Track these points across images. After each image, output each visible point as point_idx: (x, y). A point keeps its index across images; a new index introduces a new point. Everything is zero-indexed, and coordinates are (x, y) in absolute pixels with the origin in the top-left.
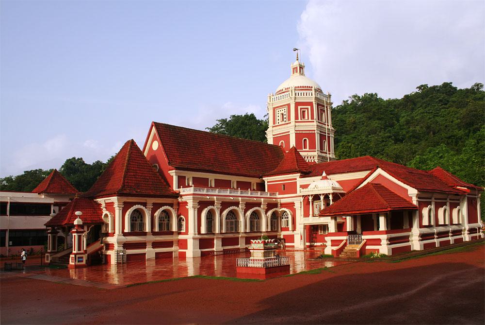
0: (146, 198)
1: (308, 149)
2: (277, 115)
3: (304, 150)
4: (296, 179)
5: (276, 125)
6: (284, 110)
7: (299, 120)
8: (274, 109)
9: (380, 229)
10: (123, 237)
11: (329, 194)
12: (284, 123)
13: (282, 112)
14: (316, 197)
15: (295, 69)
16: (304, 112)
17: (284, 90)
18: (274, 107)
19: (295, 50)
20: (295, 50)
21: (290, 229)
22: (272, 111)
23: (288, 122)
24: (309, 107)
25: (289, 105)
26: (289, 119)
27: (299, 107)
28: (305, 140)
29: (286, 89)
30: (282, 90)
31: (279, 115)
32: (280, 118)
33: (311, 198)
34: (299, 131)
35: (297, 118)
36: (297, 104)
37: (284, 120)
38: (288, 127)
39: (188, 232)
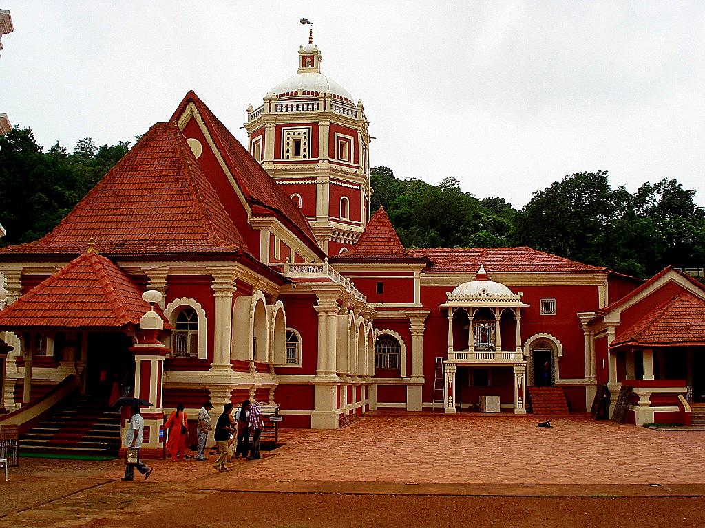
0: (259, 276)
1: (347, 220)
2: (286, 141)
3: (342, 219)
4: (412, 274)
5: (281, 160)
6: (304, 136)
7: (336, 160)
8: (278, 129)
9: (645, 378)
10: (232, 373)
11: (515, 308)
12: (300, 158)
13: (297, 136)
14: (484, 313)
15: (309, 59)
16: (342, 145)
17: (300, 95)
18: (278, 122)
19: (304, 21)
20: (304, 21)
21: (403, 373)
22: (273, 129)
23: (311, 159)
24: (352, 138)
25: (315, 127)
26: (315, 154)
27: (337, 135)
28: (344, 201)
29: (304, 93)
30: (296, 93)
31: (291, 141)
32: (291, 147)
33: (471, 316)
34: (339, 181)
35: (331, 155)
36: (334, 128)
37: (302, 153)
38: (314, 169)
39: (316, 367)
